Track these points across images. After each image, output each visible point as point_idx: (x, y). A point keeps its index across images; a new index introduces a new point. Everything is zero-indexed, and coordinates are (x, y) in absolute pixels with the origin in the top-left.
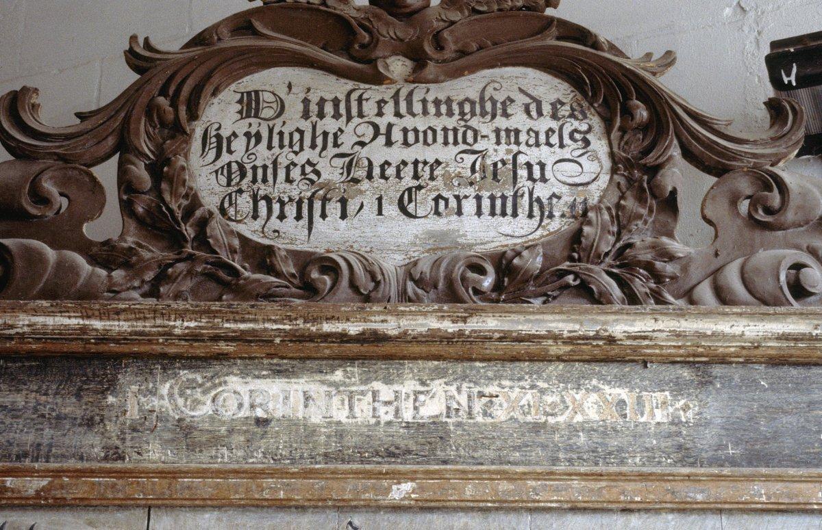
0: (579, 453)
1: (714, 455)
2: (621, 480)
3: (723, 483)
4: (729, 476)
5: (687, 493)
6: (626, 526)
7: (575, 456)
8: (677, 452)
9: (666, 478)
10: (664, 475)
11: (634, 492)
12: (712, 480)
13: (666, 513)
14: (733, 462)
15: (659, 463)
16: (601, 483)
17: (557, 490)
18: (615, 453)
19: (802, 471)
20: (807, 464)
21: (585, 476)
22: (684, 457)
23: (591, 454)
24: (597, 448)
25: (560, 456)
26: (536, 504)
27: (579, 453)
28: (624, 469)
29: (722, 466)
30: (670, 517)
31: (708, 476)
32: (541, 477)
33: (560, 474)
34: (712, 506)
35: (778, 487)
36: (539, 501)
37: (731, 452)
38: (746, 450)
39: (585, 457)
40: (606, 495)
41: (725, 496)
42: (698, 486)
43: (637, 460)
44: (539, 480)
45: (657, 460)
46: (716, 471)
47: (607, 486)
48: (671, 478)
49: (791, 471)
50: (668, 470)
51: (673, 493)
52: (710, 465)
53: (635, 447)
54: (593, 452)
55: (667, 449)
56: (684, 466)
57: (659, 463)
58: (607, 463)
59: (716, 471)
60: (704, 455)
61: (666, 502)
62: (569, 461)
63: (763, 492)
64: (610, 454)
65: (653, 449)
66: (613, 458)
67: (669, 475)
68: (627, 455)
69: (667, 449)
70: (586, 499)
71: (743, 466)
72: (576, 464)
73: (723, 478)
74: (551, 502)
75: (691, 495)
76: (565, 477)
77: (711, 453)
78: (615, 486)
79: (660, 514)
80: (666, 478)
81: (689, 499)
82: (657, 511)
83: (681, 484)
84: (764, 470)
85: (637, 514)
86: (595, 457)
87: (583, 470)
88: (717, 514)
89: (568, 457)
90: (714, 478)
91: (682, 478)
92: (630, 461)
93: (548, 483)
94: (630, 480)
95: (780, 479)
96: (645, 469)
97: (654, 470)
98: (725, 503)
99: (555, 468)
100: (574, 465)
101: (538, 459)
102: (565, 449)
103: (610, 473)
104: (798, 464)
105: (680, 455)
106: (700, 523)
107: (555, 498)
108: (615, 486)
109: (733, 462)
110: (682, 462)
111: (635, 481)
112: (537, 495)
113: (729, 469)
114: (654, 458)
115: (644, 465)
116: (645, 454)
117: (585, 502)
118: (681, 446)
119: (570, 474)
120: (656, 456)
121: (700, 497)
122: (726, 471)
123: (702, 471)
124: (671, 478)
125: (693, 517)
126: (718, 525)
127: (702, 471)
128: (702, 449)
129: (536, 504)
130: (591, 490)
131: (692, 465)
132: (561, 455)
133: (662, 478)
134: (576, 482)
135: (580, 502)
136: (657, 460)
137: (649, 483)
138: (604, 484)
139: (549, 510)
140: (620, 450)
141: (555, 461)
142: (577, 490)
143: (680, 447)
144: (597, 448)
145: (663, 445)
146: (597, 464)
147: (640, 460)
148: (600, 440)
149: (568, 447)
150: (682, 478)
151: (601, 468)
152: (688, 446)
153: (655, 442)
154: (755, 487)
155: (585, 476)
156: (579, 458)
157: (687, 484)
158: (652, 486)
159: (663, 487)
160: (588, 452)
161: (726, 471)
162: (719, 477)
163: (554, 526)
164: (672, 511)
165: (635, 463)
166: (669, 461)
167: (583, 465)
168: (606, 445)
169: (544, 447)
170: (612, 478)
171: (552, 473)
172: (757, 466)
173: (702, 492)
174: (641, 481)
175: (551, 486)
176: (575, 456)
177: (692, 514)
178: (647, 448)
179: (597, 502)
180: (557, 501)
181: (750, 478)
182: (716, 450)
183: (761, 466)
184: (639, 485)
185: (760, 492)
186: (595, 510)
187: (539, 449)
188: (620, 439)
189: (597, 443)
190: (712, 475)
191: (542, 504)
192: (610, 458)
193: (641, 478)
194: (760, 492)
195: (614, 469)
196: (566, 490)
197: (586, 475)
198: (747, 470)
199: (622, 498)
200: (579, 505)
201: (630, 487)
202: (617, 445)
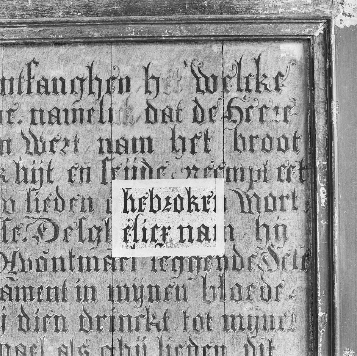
0: (27, 11)
1: (105, 9)
2: (50, 26)
3: (110, 26)
4: (112, 22)
5: (89, 32)
6: (57, 53)
7: (24, 13)
8: (84, 9)
9: (76, 24)
10: (75, 22)
11: (59, 33)
12: (103, 25)
13: (80, 45)
14: (116, 13)
15: (73, 15)
16: (40, 28)
17: (15, 33)
18: (48, 10)
19: (157, 17)
20: (159, 13)
21: (30, 24)
22: (88, 11)
23: (34, 11)
24: (38, 8)
25: (16, 13)
26: (4, 42)
27: (27, 11)
28: (52, 19)
29: (109, 16)
30: (82, 47)
31: (100, 22)
32: (5, 26)
33: (15, 23)
34: (104, 39)
35: (142, 28)
36: (5, 40)
37: (115, 7)
38: (125, 6)
39: (30, 13)
40: (43, 35)
41: (111, 33)
42: (97, 28)
43: (60, 14)
44: (5, 27)
45: (72, 14)
46: (105, 18)
47: (43, 30)
48: (80, 24)
49: (149, 18)
50: (76, 19)
51: (81, 32)
52: (103, 16)
53: (60, 6)
54: (35, 10)
55: (78, 7)
56: (87, 16)
57: (73, 15)
58: (43, 16)
59: (105, 18)
60: (100, 10)
61: (77, 38)
62: (21, 16)
63: (133, 31)
64: (45, 11)
65: (70, 7)
66: (47, 13)
67: (78, 22)
68: (55, 11)
69: (78, 7)
70: (31, 37)
71: (122, 16)
72: (25, 17)
73: (110, 23)
74: (12, 40)
75: (92, 33)
76: (18, 25)
77: (103, 9)
78: (48, 30)
79: (77, 46)
80: (76, 24)
81: (90, 36)
82: (76, 43)
83: (86, 27)
84: (133, 17)
85: (64, 47)
86: (36, 13)
87: (28, 20)
88: (110, 45)
89: (20, 13)
90: (104, 23)
91: (86, 23)
92: (56, 15)
93: (10, 29)
94: (56, 26)
95: (142, 22)
96: (63, 19)
97: (69, 19)
98: (112, 37)
99: (12, 20)
100: (24, 18)
101: (3, 15)
102: (19, 9)
103: (44, 22)
104: (154, 14)
105: (85, 10)
106: (99, 50)
107: (14, 37)
108: (48, 30)
109: (116, 13)
110: (86, 14)
111: (59, 26)
112: (3, 36)
113: (113, 17)
114: (70, 12)
115: (64, 17)
116: (65, 11)
117: (31, 39)
118: (87, 5)
119: (21, 23)
120: (72, 11)
121: (96, 35)
122: (111, 18)
123: (97, 19)
124: (80, 24)
125: (96, 47)
126: (110, 51)
127: (97, 19)
128: (99, 6)
129: (4, 42)
130: (35, 32)
131: (92, 16)
132: (17, 13)
133: (74, 24)
134: (26, 28)
135: (28, 39)
136: (72, 14)
137: (68, 28)
138: (42, 29)
139: (13, 44)
140: (51, 8)
141: (13, 16)
142: (26, 32)
143: (86, 6)
144: (38, 8)
145: (76, 4)
146: (37, 17)
147: (62, 14)
148: (40, 3)
149: (21, 8)
150: (86, 23)
151: (40, 19)
152: (90, 5)
153: (71, 3)
154: (129, 28)
155: (30, 24)
156: (27, 14)
157: (89, 27)
158: (69, 29)
159: (75, 29)
160: (33, 10)
161: (111, 18)
162: (107, 23)
163: (17, 54)
164: (84, 43)
165: (59, 16)
166: (79, 14)
167: (29, 18)
168: (43, 6)
169: (7, 8)
170: (46, 25)
171: (10, 23)
172: (130, 16)
173: (98, 32)
174: (62, 26)
175: (12, 30)
176: (24, 13)
177: (95, 45)
178: (67, 7)
179: (38, 39)
180: (15, 39)
181: (125, 23)
182: (106, 7)
183: (133, 15)
184: (62, 29)
185: (131, 31)
186: (40, 44)
187: (5, 9)
188: (51, 2)
189: (38, 5)
190: (102, 21)
191: (7, 41)
192: (45, 13)
193: (61, 24)
194: (131, 31)
195: (45, 19)
196: (20, 32)
197: (30, 23)
198: (123, 18)
199: (52, 36)
200: (28, 41)
201: (56, 30)
202: (49, 6)
